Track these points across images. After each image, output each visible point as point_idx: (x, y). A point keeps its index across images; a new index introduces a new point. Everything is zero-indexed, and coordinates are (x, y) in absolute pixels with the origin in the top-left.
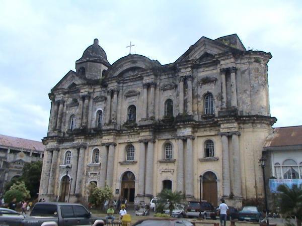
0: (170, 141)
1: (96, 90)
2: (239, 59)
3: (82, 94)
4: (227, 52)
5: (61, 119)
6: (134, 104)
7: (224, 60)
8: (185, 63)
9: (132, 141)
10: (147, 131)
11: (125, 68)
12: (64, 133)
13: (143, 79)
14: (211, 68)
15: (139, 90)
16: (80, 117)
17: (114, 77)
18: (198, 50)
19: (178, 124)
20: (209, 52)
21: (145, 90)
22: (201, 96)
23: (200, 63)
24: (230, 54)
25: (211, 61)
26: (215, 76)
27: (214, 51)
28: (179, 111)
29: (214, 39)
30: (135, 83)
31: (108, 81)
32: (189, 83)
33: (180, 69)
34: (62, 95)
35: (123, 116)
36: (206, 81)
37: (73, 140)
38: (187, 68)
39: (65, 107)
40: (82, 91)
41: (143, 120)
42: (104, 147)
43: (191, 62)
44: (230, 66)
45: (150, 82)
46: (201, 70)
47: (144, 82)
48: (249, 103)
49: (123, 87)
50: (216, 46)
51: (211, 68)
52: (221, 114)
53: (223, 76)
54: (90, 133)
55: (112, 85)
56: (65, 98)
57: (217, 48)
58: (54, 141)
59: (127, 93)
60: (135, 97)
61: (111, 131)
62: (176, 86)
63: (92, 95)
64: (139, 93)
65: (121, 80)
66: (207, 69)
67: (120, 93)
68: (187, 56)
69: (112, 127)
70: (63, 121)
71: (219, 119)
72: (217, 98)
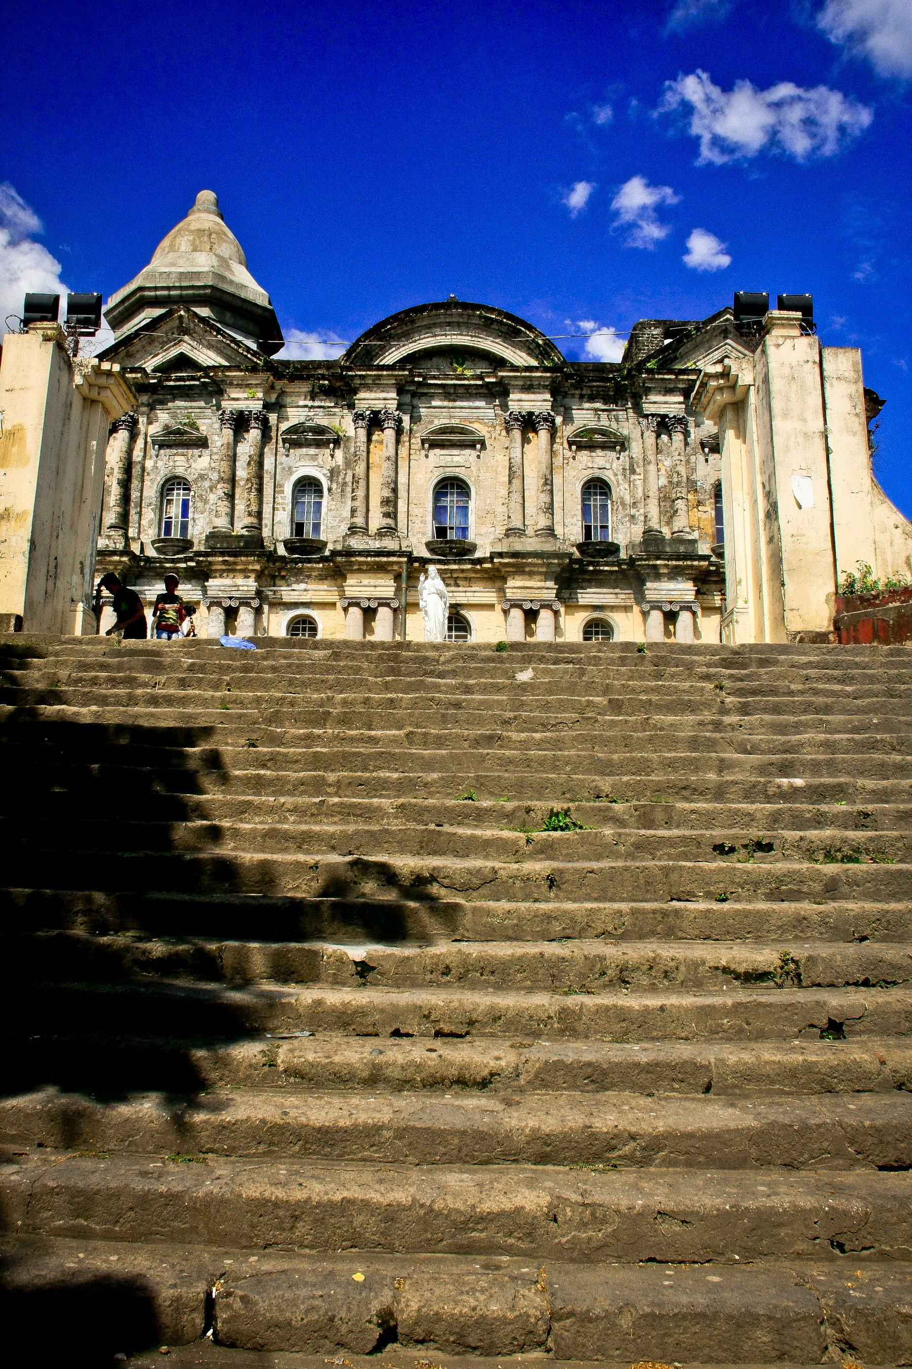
5: (125, 484)
6: (461, 473)
8: (673, 377)
10: (540, 573)
12: (142, 544)
15: (482, 430)
16: (222, 489)
19: (658, 562)
21: (517, 434)
35: (414, 510)
39: (140, 443)
41: (511, 532)
42: (355, 613)
54: (271, 556)
59: (432, 433)
60: (467, 452)
69: (389, 544)
70: (135, 495)
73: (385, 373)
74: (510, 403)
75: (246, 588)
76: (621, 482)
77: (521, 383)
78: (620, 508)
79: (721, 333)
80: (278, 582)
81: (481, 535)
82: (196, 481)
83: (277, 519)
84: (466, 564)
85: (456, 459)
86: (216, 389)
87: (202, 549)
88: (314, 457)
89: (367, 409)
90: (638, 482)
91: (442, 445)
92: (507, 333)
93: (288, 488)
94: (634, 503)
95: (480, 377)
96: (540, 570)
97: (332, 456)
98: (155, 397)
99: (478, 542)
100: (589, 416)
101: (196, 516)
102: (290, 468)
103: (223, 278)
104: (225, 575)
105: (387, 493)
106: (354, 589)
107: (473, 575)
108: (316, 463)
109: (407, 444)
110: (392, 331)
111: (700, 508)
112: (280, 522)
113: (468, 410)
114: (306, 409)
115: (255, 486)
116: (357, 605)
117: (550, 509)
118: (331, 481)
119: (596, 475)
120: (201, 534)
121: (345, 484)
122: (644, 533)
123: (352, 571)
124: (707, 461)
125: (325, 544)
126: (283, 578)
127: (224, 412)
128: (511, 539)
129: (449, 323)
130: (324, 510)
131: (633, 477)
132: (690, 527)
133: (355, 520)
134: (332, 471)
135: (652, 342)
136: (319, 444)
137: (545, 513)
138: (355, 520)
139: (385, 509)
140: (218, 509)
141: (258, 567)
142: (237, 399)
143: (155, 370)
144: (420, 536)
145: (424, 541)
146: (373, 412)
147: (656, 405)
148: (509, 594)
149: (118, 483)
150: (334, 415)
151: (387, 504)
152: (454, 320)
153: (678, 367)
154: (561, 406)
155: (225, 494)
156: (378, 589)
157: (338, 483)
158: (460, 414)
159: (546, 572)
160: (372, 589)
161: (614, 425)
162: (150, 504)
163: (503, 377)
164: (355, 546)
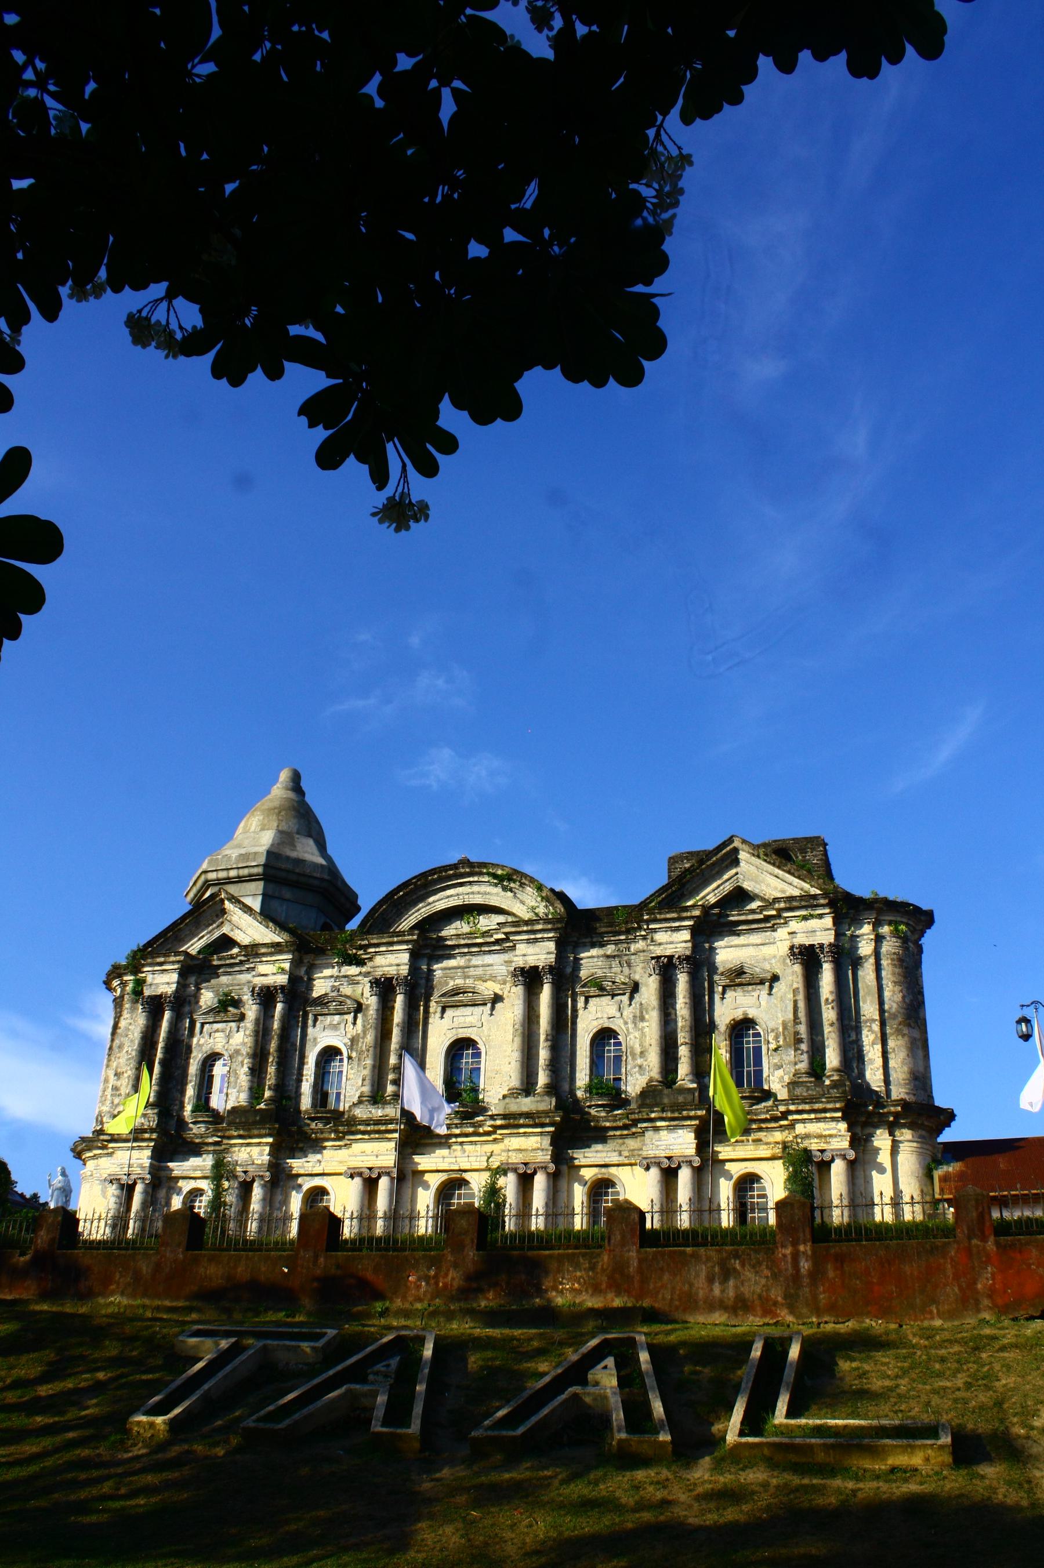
0: (613, 1170)
2: (848, 920)
4: (814, 897)
9: (465, 1166)
13: (513, 948)
14: (755, 938)
17: (401, 934)
20: (747, 885)
24: (822, 901)
26: (767, 967)
30: (476, 961)
32: (682, 980)
33: (655, 931)
36: (739, 977)
38: (677, 929)
41: (513, 1094)
45: (541, 964)
47: (519, 962)
48: (879, 1062)
52: (799, 1091)
55: (391, 959)
58: (140, 1148)
60: (481, 1008)
61: (391, 1127)
62: (635, 988)
71: (792, 1108)
72: (776, 1038)
73: (395, 939)
75: (259, 1162)
76: (631, 1030)
78: (630, 1058)
84: (467, 1127)
88: (335, 1027)
94: (642, 1053)
97: (354, 1024)
100: (600, 963)
102: (315, 1039)
104: (243, 1148)
108: (338, 1033)
113: (481, 968)
114: (333, 980)
116: (360, 1174)
118: (352, 1050)
119: (606, 1025)
124: (723, 998)
125: (343, 1113)
127: (254, 988)
128: (507, 1100)
131: (641, 1025)
146: (386, 979)
147: (662, 947)
149: (159, 1063)
150: (358, 983)
155: (249, 1068)
156: (380, 1158)
157: (357, 1051)
159: (541, 1132)
161: (626, 970)
162: (191, 1081)
163: (505, 933)
164: (359, 1116)
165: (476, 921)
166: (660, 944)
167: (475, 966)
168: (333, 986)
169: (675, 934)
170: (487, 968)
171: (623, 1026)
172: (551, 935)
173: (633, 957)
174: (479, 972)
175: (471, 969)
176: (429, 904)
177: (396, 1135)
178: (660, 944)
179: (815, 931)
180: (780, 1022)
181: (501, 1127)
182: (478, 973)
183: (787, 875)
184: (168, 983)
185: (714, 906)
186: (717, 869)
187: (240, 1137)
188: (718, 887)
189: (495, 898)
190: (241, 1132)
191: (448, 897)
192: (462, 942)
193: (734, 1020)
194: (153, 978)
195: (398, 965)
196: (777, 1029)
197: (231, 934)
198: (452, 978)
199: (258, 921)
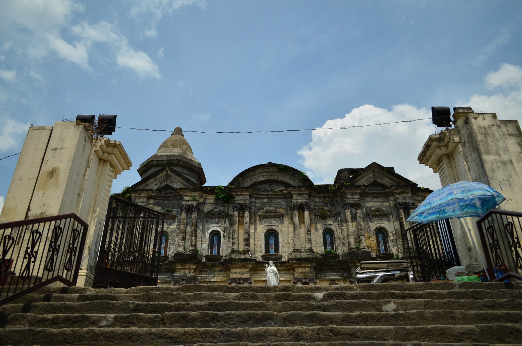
1: (208, 201)
3: (187, 203)
5: (142, 234)
6: (275, 228)
7: (400, 193)
10: (308, 267)
11: (261, 179)
13: (291, 197)
15: (282, 211)
18: (365, 176)
20: (378, 180)
22: (372, 231)
23: (369, 191)
25: (382, 192)
27: (386, 181)
28: (349, 244)
29: (364, 167)
31: (236, 192)
33: (346, 194)
34: (145, 200)
37: (174, 271)
38: (355, 194)
40: (186, 198)
41: (295, 251)
43: (363, 188)
44: (409, 201)
46: (368, 199)
49: (256, 203)
50: (390, 176)
51: (380, 200)
53: (402, 212)
56: (149, 204)
57: (390, 178)
59: (263, 212)
60: (278, 219)
63: (202, 208)
64: (283, 216)
65: (255, 194)
66: (376, 200)
67: (253, 210)
68: (354, 181)
72: (393, 235)
74: (293, 200)
75: (190, 276)
77: (296, 193)
79: (372, 172)
80: (203, 273)
81: (284, 252)
82: (171, 233)
83: (203, 247)
85: (272, 222)
86: (180, 197)
87: (172, 260)
88: (218, 223)
89: (238, 204)
90: (345, 229)
91: (267, 217)
92: (291, 175)
93: (207, 235)
94: (344, 238)
95: (281, 191)
96: (308, 265)
97: (225, 222)
98: (156, 201)
99: (283, 255)
101: (170, 247)
102: (208, 227)
103: (184, 157)
104: (181, 270)
105: (246, 236)
106: (234, 275)
107: (281, 268)
108: (218, 225)
109: (254, 217)
110: (247, 175)
111: (370, 239)
112: (204, 249)
113: (277, 204)
115: (194, 234)
117: (310, 241)
118: (224, 232)
120: (172, 254)
121: (230, 233)
122: (348, 250)
123: (233, 268)
125: (222, 257)
126: (205, 271)
127: (183, 206)
128: (296, 253)
129: (269, 171)
130: (222, 243)
131: (342, 228)
132: (367, 247)
133: (234, 247)
134: (225, 228)
135: (345, 177)
136: (219, 218)
137: (308, 242)
138: (234, 247)
139: (245, 243)
140: (180, 244)
141: (195, 267)
142: (188, 201)
143: (157, 190)
144: (259, 253)
145: (261, 255)
146: (240, 205)
148: (296, 275)
150: (225, 206)
151: (246, 241)
152: (270, 170)
153: (356, 184)
154: (313, 201)
155: (182, 237)
158: (274, 205)
159: (310, 266)
160: (241, 275)
163: (290, 191)
164: (234, 258)
165: (273, 186)
166: (349, 199)
167: (275, 203)
168: (215, 207)
169: (354, 196)
170: (279, 204)
171: (335, 229)
172: (307, 193)
173: (336, 203)
174: (276, 205)
175: (273, 204)
176: (256, 178)
177: (250, 266)
178: (349, 199)
179: (406, 198)
180: (394, 229)
181: (295, 264)
182: (275, 205)
183: (394, 178)
184: (142, 202)
185: (366, 187)
186: (367, 174)
187: (181, 265)
188: (368, 180)
189: (282, 178)
190: (182, 263)
191: (264, 176)
192: (270, 193)
193: (376, 228)
194: (135, 200)
195: (245, 200)
196: (393, 232)
197: (170, 184)
198: (265, 207)
199: (184, 180)
